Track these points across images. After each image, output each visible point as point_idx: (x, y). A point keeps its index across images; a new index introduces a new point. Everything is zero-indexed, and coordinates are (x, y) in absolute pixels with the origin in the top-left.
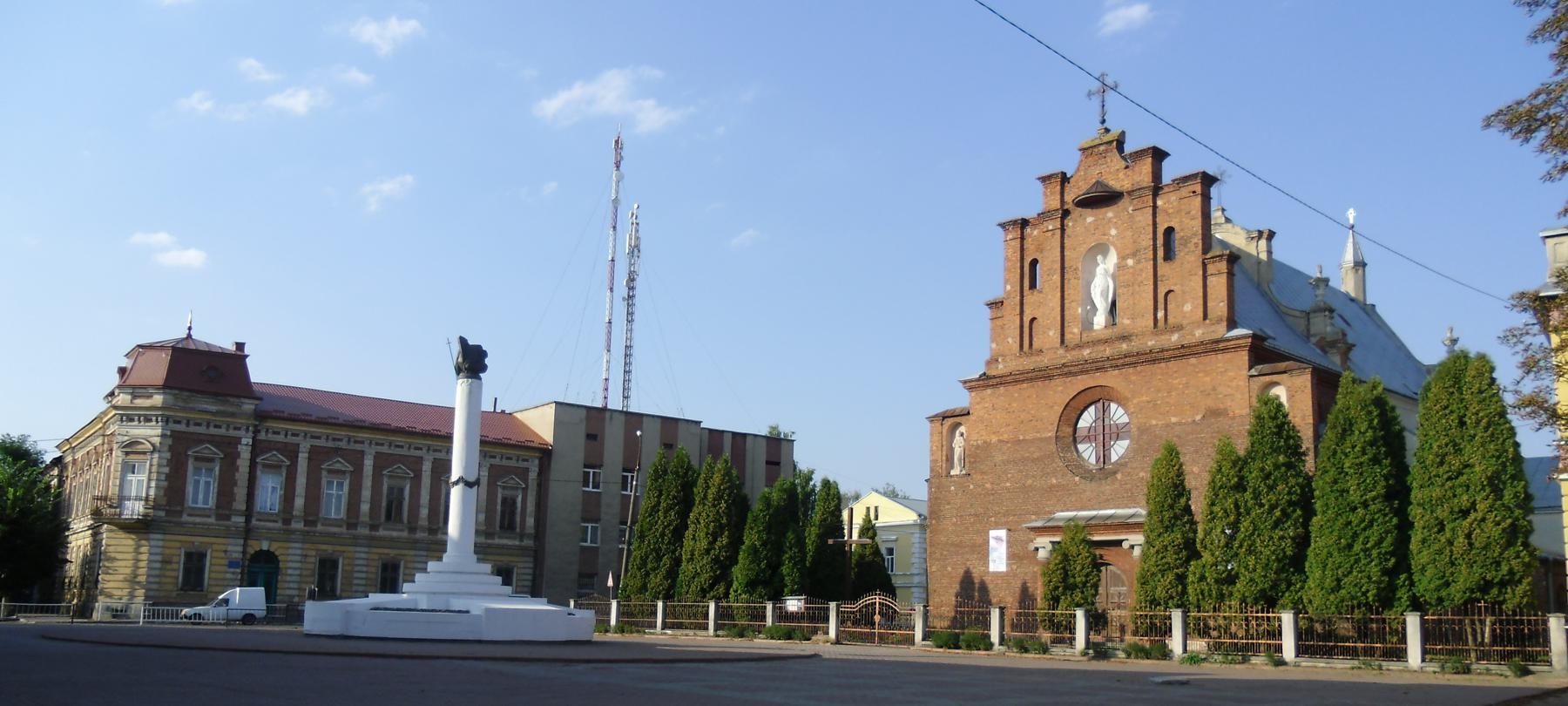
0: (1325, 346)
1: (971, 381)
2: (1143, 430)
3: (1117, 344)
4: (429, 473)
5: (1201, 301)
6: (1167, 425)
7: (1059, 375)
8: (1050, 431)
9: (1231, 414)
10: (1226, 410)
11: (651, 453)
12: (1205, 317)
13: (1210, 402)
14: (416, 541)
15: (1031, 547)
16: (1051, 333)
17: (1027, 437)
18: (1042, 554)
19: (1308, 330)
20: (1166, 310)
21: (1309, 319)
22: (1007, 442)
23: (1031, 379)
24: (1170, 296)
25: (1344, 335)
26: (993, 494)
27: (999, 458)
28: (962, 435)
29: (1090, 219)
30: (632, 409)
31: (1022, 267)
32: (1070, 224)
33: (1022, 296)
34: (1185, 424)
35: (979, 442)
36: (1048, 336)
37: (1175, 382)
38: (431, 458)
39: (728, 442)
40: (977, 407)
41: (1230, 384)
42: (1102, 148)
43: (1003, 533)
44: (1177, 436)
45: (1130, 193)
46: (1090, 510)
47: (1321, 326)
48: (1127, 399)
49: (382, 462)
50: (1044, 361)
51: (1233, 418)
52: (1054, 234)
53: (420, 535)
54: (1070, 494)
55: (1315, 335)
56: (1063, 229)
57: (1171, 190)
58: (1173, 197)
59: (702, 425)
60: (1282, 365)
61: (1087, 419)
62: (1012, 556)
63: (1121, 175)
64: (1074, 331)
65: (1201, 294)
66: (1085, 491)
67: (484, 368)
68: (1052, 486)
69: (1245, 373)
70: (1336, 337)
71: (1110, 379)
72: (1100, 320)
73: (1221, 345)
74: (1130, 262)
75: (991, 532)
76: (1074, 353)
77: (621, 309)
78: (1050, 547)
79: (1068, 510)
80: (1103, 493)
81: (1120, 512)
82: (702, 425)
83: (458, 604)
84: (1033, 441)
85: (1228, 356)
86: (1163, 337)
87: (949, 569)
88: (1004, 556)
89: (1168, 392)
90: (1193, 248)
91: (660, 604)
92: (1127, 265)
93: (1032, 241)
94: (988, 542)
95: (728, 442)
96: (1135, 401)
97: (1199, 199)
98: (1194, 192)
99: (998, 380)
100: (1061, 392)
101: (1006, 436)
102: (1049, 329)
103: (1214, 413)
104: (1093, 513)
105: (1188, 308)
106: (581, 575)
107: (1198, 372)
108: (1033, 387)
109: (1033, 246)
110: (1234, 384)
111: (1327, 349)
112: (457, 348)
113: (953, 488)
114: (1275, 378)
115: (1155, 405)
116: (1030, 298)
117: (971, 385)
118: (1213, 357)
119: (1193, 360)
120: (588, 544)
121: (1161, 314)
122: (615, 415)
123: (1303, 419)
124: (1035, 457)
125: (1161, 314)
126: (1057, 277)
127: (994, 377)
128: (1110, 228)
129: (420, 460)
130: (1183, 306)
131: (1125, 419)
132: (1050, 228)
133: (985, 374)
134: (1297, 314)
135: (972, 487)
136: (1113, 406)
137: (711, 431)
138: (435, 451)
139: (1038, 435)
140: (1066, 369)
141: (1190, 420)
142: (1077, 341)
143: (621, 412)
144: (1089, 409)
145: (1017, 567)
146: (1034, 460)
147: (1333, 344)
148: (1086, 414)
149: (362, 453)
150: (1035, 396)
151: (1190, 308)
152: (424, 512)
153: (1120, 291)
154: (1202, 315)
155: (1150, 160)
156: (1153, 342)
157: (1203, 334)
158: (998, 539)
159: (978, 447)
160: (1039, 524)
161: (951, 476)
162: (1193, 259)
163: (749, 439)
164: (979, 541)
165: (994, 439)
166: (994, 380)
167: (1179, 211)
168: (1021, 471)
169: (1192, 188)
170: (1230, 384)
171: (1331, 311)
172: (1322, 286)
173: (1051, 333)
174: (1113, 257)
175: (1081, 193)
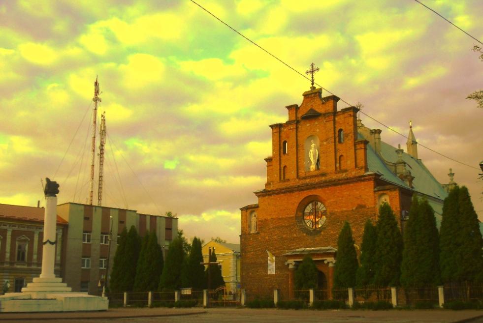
0: (403, 178)
1: (259, 193)
2: (332, 214)
4: (10, 237)
5: (354, 160)
6: (342, 212)
9: (367, 207)
11: (115, 227)
12: (356, 166)
13: (359, 202)
14: (31, 270)
15: (286, 264)
18: (291, 267)
19: (396, 171)
20: (340, 163)
21: (396, 166)
23: (285, 192)
24: (342, 158)
25: (410, 173)
27: (271, 226)
28: (255, 216)
29: (308, 125)
30: (103, 205)
31: (280, 145)
32: (300, 126)
33: (280, 156)
34: (349, 211)
36: (291, 174)
38: (11, 230)
39: (148, 220)
40: (262, 204)
42: (312, 95)
44: (346, 216)
45: (324, 115)
46: (310, 247)
47: (401, 169)
48: (325, 200)
49: (15, 235)
50: (290, 184)
51: (368, 208)
52: (293, 131)
53: (6, 266)
55: (399, 173)
56: (297, 128)
58: (342, 116)
59: (137, 212)
60: (388, 187)
61: (309, 209)
62: (277, 268)
63: (321, 107)
64: (302, 173)
65: (354, 157)
66: (308, 240)
67: (58, 192)
68: (294, 238)
69: (372, 190)
70: (407, 174)
71: (318, 192)
72: (313, 167)
73: (363, 178)
74: (325, 143)
77: (97, 159)
78: (294, 263)
79: (301, 248)
81: (323, 248)
82: (137, 212)
83: (50, 296)
84: (285, 219)
85: (366, 183)
87: (251, 274)
88: (274, 268)
90: (350, 138)
95: (148, 220)
96: (328, 201)
97: (352, 118)
98: (350, 115)
100: (298, 198)
101: (274, 217)
103: (361, 207)
105: (349, 162)
106: (82, 282)
108: (285, 195)
111: (404, 179)
112: (45, 182)
113: (251, 239)
114: (385, 192)
116: (284, 157)
117: (260, 194)
118: (359, 184)
119: (351, 185)
120: (85, 268)
121: (338, 165)
122: (97, 208)
123: (396, 209)
125: (338, 165)
126: (295, 149)
127: (269, 191)
129: (6, 231)
130: (347, 162)
131: (324, 209)
132: (292, 128)
133: (265, 190)
134: (392, 164)
135: (260, 238)
137: (141, 215)
138: (13, 226)
140: (299, 188)
141: (351, 209)
142: (304, 176)
143: (98, 207)
147: (406, 177)
148: (308, 207)
149: (34, 233)
152: (35, 257)
153: (321, 155)
154: (354, 165)
155: (332, 101)
160: (289, 254)
161: (251, 234)
162: (350, 142)
163: (158, 218)
164: (263, 261)
165: (269, 218)
167: (344, 123)
169: (349, 113)
171: (405, 163)
172: (401, 153)
173: (293, 173)
175: (304, 114)
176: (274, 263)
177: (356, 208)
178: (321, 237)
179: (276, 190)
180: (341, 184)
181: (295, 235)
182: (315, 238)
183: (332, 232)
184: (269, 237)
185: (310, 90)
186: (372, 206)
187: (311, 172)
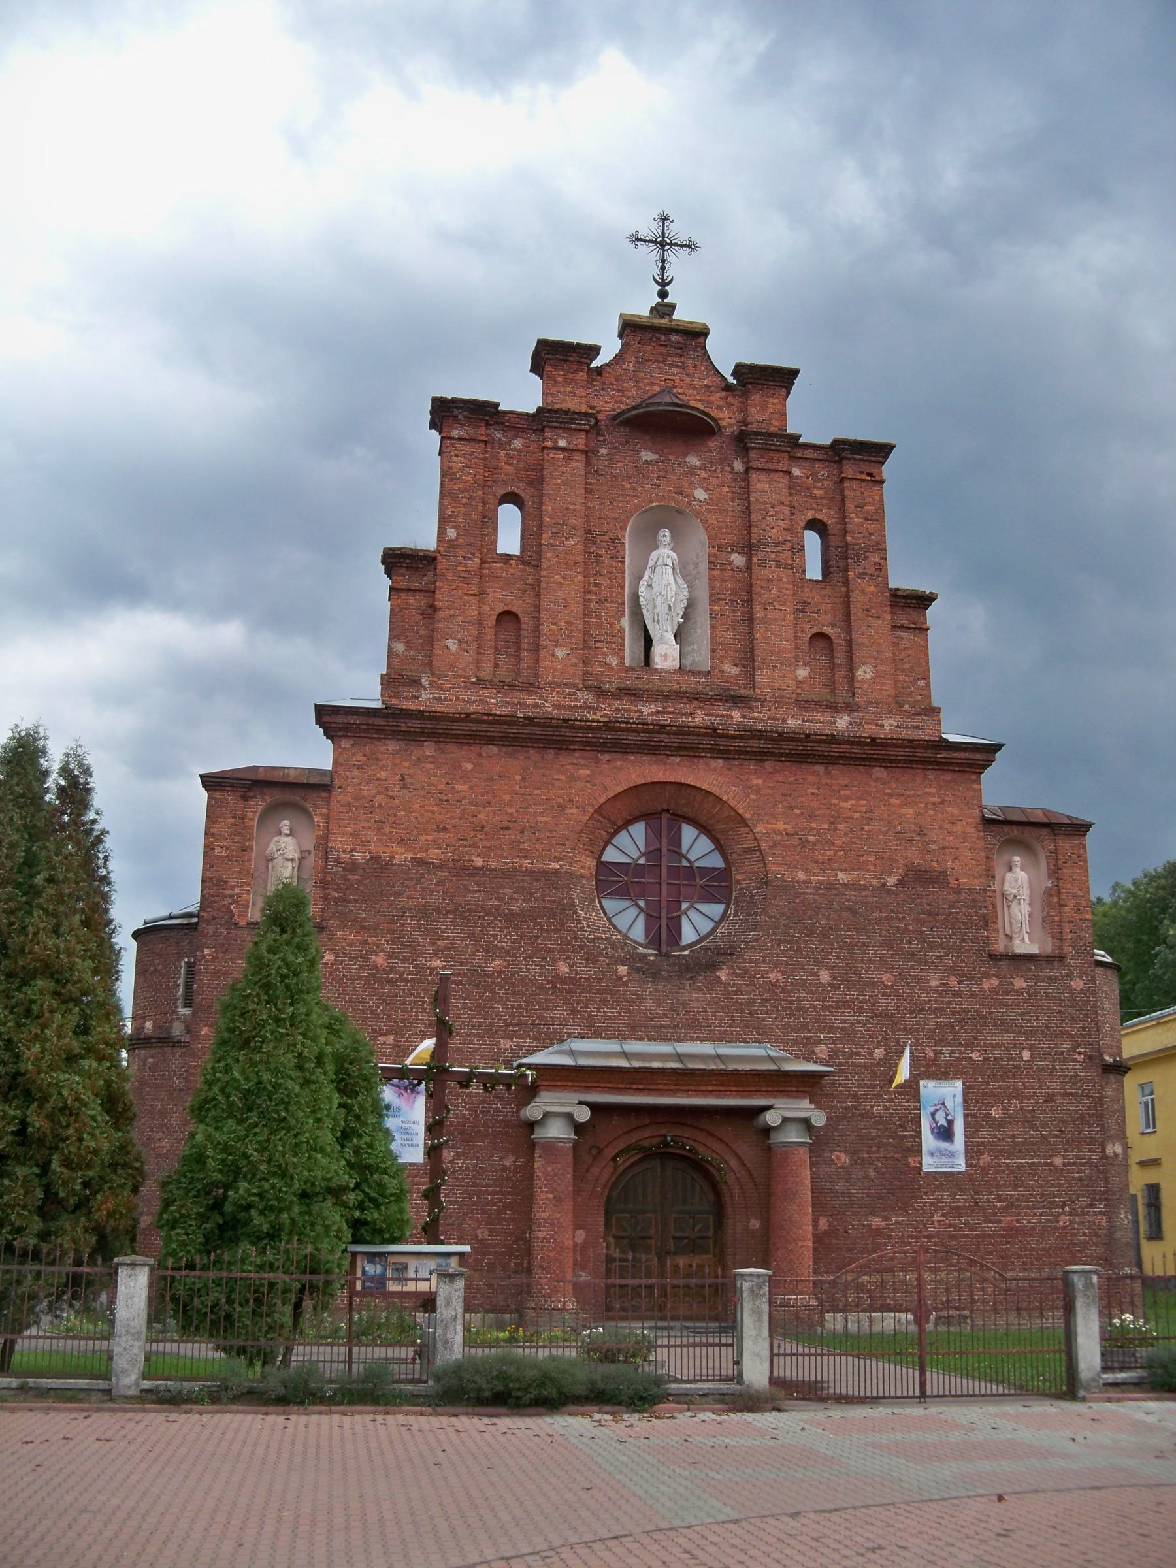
3: (720, 709)
6: (831, 886)
7: (588, 743)
8: (556, 859)
9: (953, 884)
10: (944, 874)
13: (913, 855)
16: (560, 653)
17: (494, 864)
22: (440, 867)
26: (390, 981)
32: (603, 451)
34: (865, 888)
35: (358, 856)
37: (843, 804)
40: (356, 773)
41: (949, 826)
42: (675, 338)
44: (849, 909)
50: (548, 706)
51: (958, 891)
52: (569, 458)
54: (605, 1000)
57: (821, 457)
68: (560, 978)
76: (617, 704)
79: (597, 1035)
80: (684, 1005)
84: (509, 875)
85: (948, 777)
89: (831, 823)
92: (730, 564)
93: (508, 456)
101: (434, 854)
102: (557, 645)
104: (707, 1048)
107: (890, 795)
109: (508, 469)
110: (958, 828)
115: (803, 843)
119: (879, 772)
124: (515, 909)
128: (693, 486)
132: (562, 443)
136: (688, 833)
139: (526, 863)
144: (631, 828)
145: (457, 1156)
146: (509, 917)
150: (518, 777)
151: (868, 676)
156: (799, 722)
157: (898, 727)
159: (353, 867)
165: (402, 855)
166: (418, 724)
168: (471, 935)
170: (949, 826)
173: (560, 653)
174: (699, 544)
177: (901, 882)
178: (717, 993)
180: (829, 760)
181: (563, 968)
182: (685, 997)
183: (774, 976)
184: (390, 957)
185: (646, 312)
186: (977, 883)
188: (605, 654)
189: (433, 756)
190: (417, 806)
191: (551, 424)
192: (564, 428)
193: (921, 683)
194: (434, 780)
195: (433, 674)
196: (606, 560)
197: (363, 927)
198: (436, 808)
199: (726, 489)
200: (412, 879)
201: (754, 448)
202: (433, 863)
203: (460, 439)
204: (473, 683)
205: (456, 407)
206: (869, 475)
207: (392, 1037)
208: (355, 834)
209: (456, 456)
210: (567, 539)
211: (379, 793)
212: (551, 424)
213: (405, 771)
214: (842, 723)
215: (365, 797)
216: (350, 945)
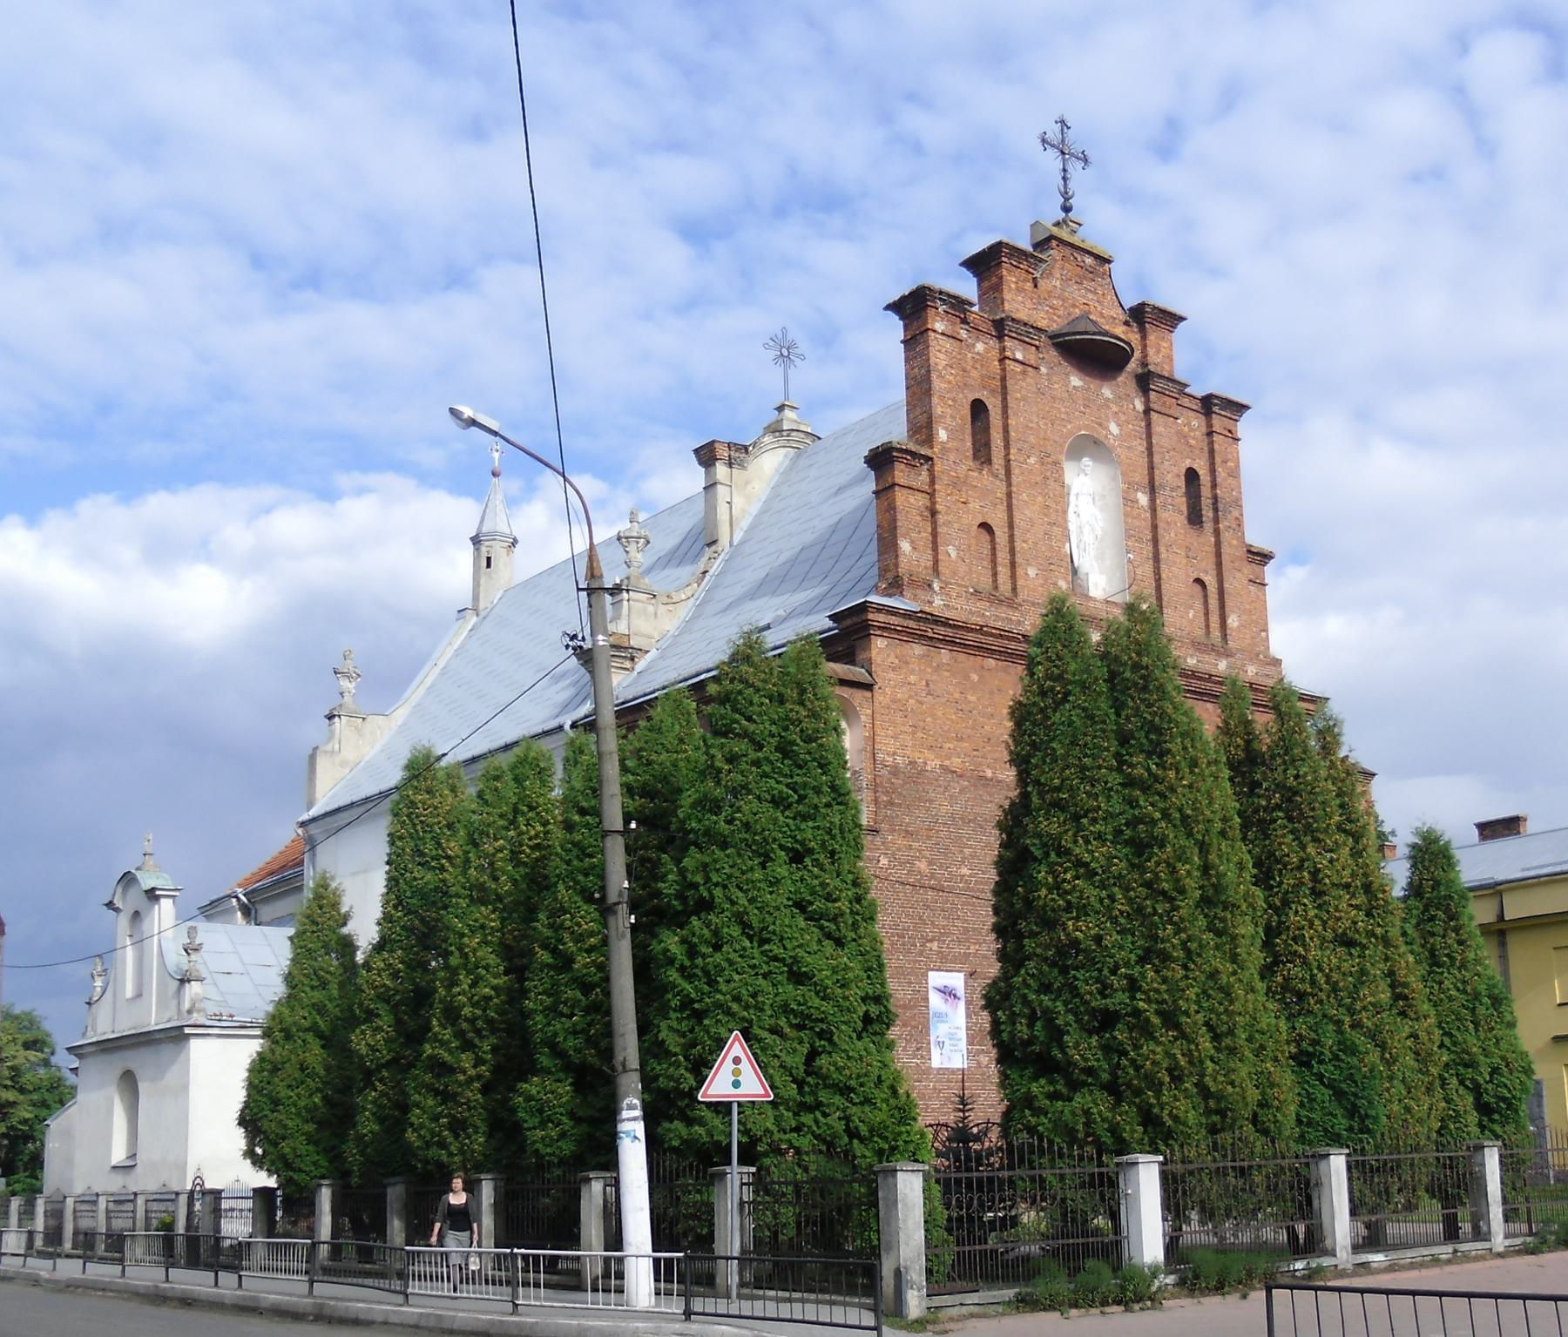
35: (899, 760)
40: (891, 675)
43: (957, 980)
57: (1194, 407)
75: (930, 973)
86: (1207, 658)
88: (963, 1034)
91: (1338, 1164)
92: (1137, 501)
94: (926, 1000)
99: (950, 632)
101: (955, 763)
108: (1005, 670)
132: (1019, 356)
135: (884, 861)
158: (948, 993)
159: (895, 772)
165: (933, 764)
166: (942, 630)
176: (962, 1005)
179: (980, 630)
184: (930, 863)
187: (1095, 600)
188: (1056, 577)
189: (948, 664)
190: (939, 713)
191: (1011, 334)
192: (1020, 340)
193: (1263, 634)
194: (951, 689)
195: (941, 581)
196: (1051, 482)
197: (907, 832)
198: (954, 717)
199: (1130, 426)
200: (940, 786)
201: (1153, 390)
202: (955, 772)
203: (943, 334)
204: (972, 594)
205: (940, 299)
206: (1230, 431)
207: (936, 943)
208: (895, 737)
209: (939, 351)
210: (1029, 457)
211: (910, 697)
212: (1011, 334)
213: (928, 677)
214: (1222, 666)
215: (899, 700)
216: (899, 850)
